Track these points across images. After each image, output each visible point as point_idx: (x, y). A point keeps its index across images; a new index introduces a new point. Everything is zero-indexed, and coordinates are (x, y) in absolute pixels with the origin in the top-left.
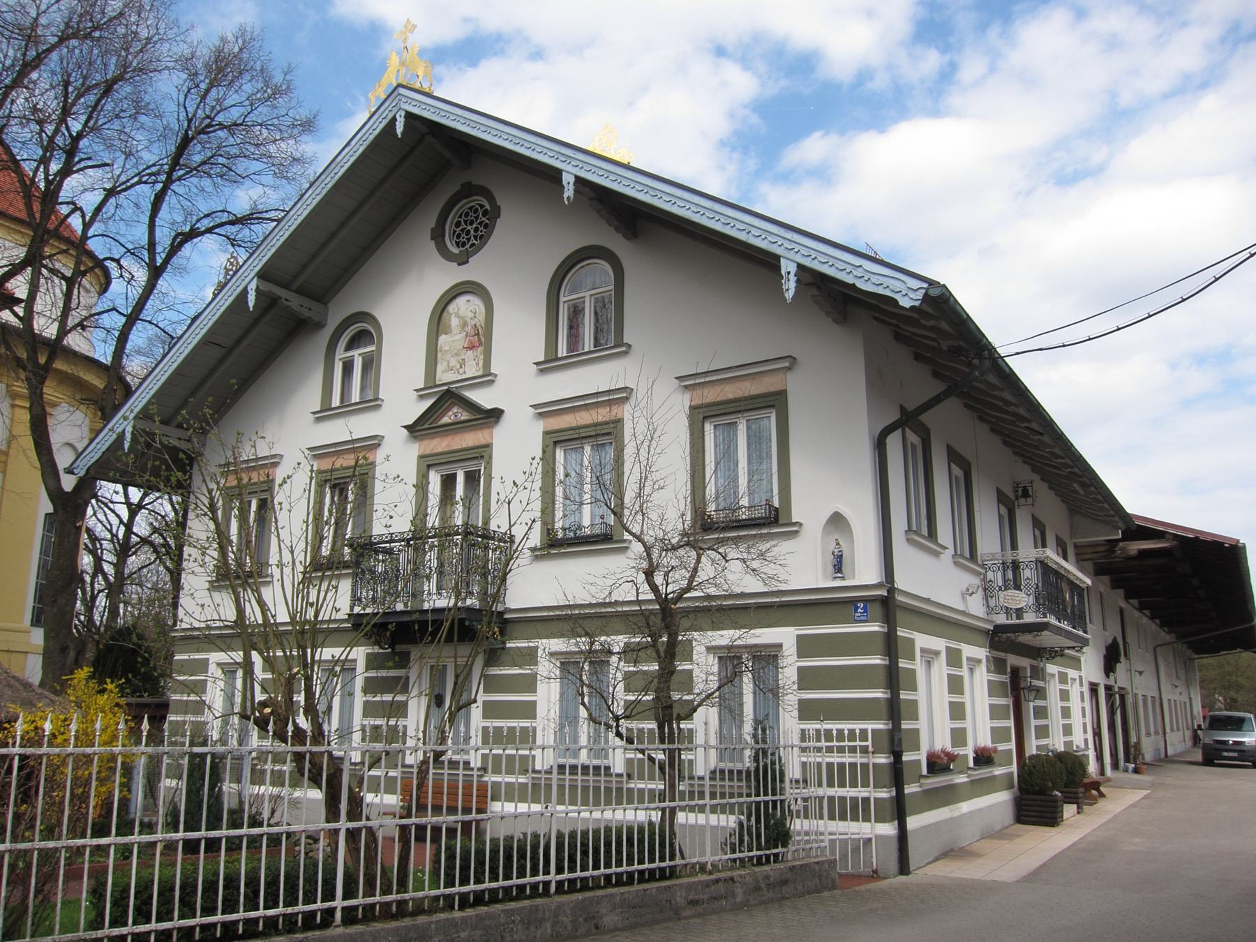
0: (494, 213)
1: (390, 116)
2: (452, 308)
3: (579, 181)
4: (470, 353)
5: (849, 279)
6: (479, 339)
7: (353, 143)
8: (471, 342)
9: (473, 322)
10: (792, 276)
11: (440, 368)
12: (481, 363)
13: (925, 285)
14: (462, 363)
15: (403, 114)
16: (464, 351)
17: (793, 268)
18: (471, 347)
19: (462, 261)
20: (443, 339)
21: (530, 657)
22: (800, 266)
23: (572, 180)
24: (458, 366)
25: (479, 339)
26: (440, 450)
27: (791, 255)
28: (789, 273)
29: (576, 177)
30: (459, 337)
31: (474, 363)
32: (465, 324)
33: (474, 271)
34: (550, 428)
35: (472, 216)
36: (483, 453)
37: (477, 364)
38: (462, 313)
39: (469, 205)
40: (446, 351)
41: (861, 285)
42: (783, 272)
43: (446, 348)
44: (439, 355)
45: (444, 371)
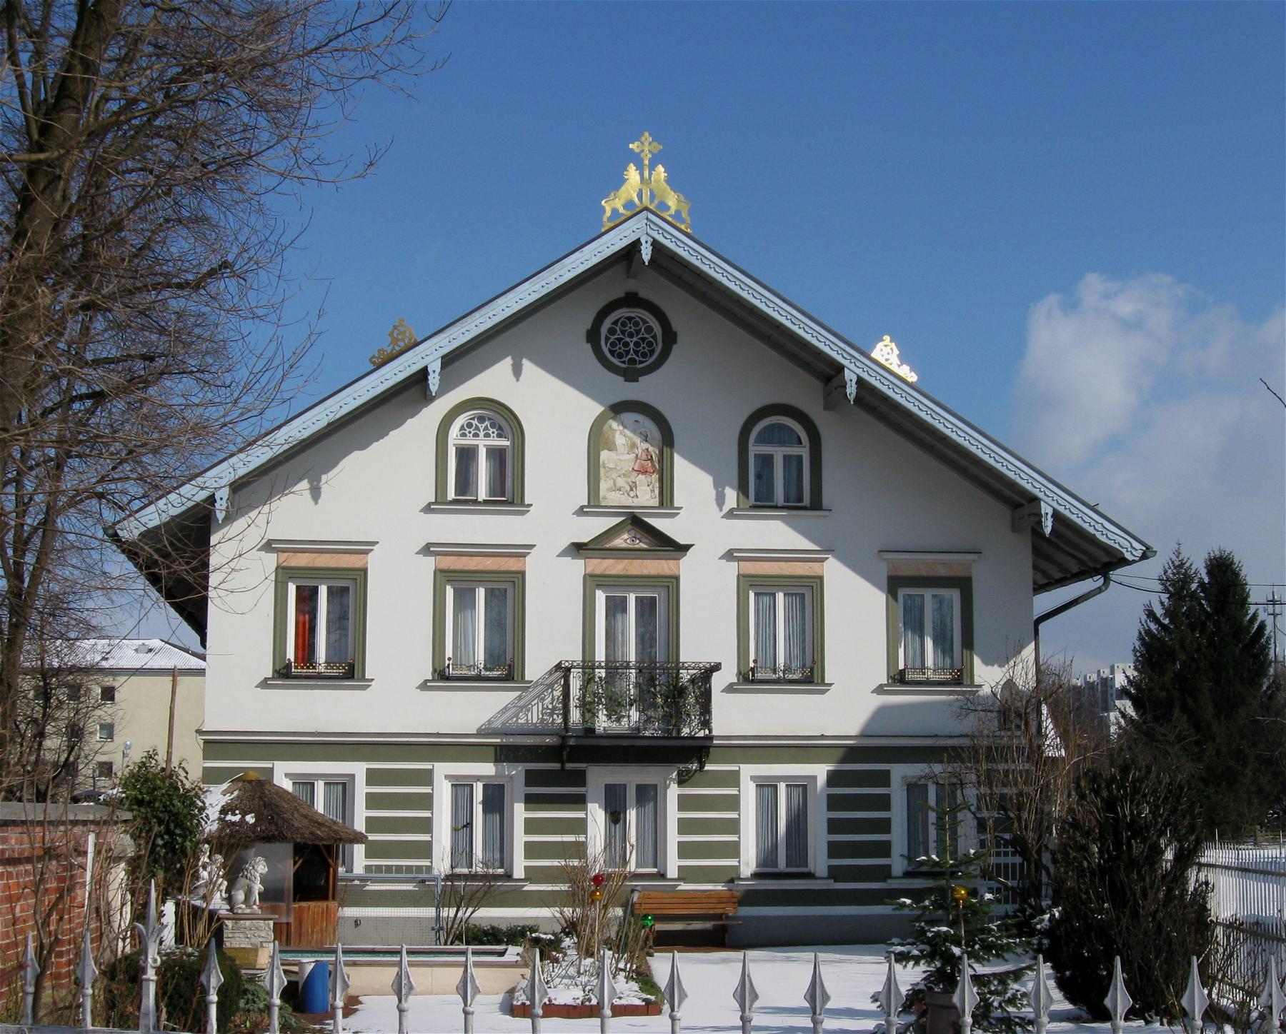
0: (670, 338)
1: (632, 238)
3: (861, 382)
4: (641, 477)
5: (1091, 530)
8: (642, 466)
10: (1049, 516)
11: (604, 486)
12: (657, 491)
13: (1144, 549)
14: (633, 487)
16: (635, 474)
17: (1050, 511)
18: (643, 471)
19: (631, 375)
20: (605, 455)
21: (733, 780)
22: (1054, 510)
23: (855, 379)
24: (628, 489)
26: (614, 572)
27: (1049, 500)
28: (1047, 514)
29: (859, 377)
30: (627, 457)
34: (747, 572)
36: (671, 584)
37: (653, 491)
39: (627, 315)
41: (1098, 535)
42: (1043, 512)
43: (612, 466)
44: (602, 471)
45: (610, 490)
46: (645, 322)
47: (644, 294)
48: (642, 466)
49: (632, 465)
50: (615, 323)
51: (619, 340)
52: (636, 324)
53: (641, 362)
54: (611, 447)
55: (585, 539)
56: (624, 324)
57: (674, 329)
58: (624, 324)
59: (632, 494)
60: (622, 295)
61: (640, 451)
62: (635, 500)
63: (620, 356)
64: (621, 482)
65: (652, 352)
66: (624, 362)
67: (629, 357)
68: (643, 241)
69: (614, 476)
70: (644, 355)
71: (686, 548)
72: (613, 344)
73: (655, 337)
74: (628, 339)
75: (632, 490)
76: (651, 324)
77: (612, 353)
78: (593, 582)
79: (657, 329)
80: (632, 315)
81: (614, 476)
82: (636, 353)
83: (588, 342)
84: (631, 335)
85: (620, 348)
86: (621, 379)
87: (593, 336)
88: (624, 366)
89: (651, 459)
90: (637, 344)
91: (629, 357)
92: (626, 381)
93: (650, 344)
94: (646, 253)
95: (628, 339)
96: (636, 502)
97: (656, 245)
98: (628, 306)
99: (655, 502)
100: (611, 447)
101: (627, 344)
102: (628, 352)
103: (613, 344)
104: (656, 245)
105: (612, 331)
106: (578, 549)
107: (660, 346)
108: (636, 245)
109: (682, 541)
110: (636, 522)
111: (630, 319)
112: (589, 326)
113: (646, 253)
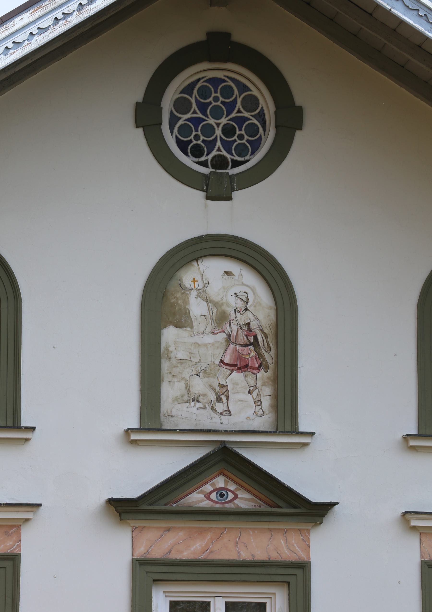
6: (259, 355)
8: (239, 357)
9: (242, 319)
12: (266, 402)
16: (225, 370)
24: (212, 397)
25: (259, 355)
30: (209, 339)
31: (250, 398)
37: (258, 403)
40: (181, 361)
43: (181, 355)
44: (165, 365)
45: (177, 400)
46: (243, 88)
48: (239, 357)
51: (196, 121)
53: (236, 164)
57: (299, 101)
59: (220, 407)
60: (201, 37)
61: (235, 328)
62: (225, 418)
66: (204, 164)
67: (214, 153)
69: (187, 373)
73: (261, 117)
74: (212, 121)
75: (219, 400)
76: (255, 92)
80: (220, 75)
81: (187, 373)
83: (137, 126)
86: (202, 194)
89: (255, 344)
91: (214, 153)
92: (208, 198)
95: (212, 121)
98: (211, 60)
107: (272, 133)
111: (215, 82)
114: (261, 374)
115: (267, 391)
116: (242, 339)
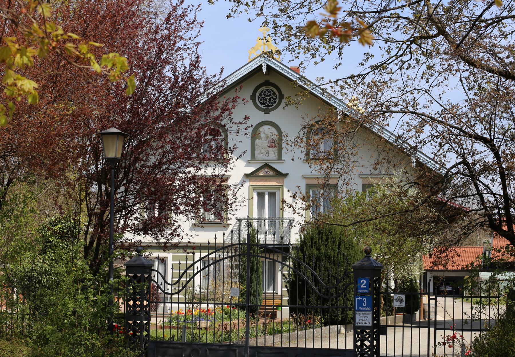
0: (281, 97)
1: (259, 64)
2: (261, 129)
6: (275, 144)
7: (242, 69)
9: (272, 137)
11: (257, 152)
12: (276, 154)
14: (268, 152)
15: (266, 65)
18: (271, 147)
19: (267, 112)
20: (257, 141)
25: (275, 144)
30: (265, 142)
32: (268, 137)
33: (272, 116)
34: (309, 183)
35: (267, 94)
37: (275, 154)
38: (266, 132)
44: (256, 147)
46: (273, 91)
47: (272, 81)
49: (267, 144)
50: (262, 92)
51: (263, 98)
52: (269, 92)
54: (260, 138)
55: (249, 172)
56: (265, 92)
58: (265, 92)
63: (264, 104)
64: (263, 151)
65: (275, 102)
66: (265, 106)
68: (263, 65)
69: (260, 148)
70: (272, 103)
71: (286, 175)
72: (261, 100)
73: (276, 97)
77: (261, 103)
78: (254, 188)
79: (277, 94)
81: (260, 148)
82: (270, 102)
84: (267, 96)
85: (263, 101)
87: (253, 98)
88: (264, 108)
89: (274, 142)
90: (270, 99)
93: (274, 99)
94: (264, 69)
96: (269, 158)
97: (268, 66)
99: (276, 158)
100: (260, 138)
101: (266, 100)
102: (266, 102)
103: (261, 100)
104: (268, 66)
105: (260, 95)
106: (247, 176)
108: (261, 65)
109: (284, 172)
110: (266, 165)
111: (267, 90)
112: (251, 94)
113: (264, 69)
114: (275, 148)
115: (277, 151)
116: (272, 141)
